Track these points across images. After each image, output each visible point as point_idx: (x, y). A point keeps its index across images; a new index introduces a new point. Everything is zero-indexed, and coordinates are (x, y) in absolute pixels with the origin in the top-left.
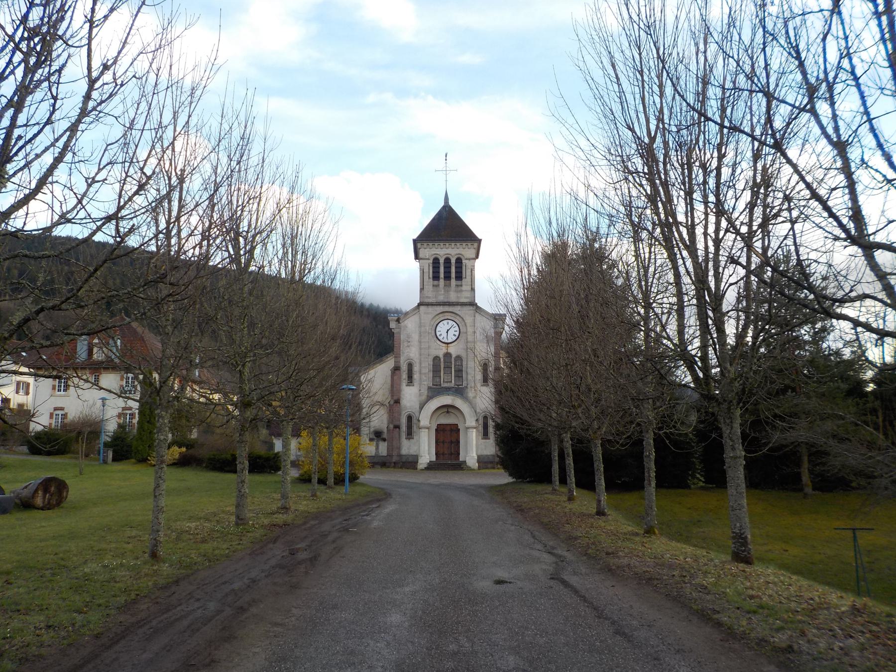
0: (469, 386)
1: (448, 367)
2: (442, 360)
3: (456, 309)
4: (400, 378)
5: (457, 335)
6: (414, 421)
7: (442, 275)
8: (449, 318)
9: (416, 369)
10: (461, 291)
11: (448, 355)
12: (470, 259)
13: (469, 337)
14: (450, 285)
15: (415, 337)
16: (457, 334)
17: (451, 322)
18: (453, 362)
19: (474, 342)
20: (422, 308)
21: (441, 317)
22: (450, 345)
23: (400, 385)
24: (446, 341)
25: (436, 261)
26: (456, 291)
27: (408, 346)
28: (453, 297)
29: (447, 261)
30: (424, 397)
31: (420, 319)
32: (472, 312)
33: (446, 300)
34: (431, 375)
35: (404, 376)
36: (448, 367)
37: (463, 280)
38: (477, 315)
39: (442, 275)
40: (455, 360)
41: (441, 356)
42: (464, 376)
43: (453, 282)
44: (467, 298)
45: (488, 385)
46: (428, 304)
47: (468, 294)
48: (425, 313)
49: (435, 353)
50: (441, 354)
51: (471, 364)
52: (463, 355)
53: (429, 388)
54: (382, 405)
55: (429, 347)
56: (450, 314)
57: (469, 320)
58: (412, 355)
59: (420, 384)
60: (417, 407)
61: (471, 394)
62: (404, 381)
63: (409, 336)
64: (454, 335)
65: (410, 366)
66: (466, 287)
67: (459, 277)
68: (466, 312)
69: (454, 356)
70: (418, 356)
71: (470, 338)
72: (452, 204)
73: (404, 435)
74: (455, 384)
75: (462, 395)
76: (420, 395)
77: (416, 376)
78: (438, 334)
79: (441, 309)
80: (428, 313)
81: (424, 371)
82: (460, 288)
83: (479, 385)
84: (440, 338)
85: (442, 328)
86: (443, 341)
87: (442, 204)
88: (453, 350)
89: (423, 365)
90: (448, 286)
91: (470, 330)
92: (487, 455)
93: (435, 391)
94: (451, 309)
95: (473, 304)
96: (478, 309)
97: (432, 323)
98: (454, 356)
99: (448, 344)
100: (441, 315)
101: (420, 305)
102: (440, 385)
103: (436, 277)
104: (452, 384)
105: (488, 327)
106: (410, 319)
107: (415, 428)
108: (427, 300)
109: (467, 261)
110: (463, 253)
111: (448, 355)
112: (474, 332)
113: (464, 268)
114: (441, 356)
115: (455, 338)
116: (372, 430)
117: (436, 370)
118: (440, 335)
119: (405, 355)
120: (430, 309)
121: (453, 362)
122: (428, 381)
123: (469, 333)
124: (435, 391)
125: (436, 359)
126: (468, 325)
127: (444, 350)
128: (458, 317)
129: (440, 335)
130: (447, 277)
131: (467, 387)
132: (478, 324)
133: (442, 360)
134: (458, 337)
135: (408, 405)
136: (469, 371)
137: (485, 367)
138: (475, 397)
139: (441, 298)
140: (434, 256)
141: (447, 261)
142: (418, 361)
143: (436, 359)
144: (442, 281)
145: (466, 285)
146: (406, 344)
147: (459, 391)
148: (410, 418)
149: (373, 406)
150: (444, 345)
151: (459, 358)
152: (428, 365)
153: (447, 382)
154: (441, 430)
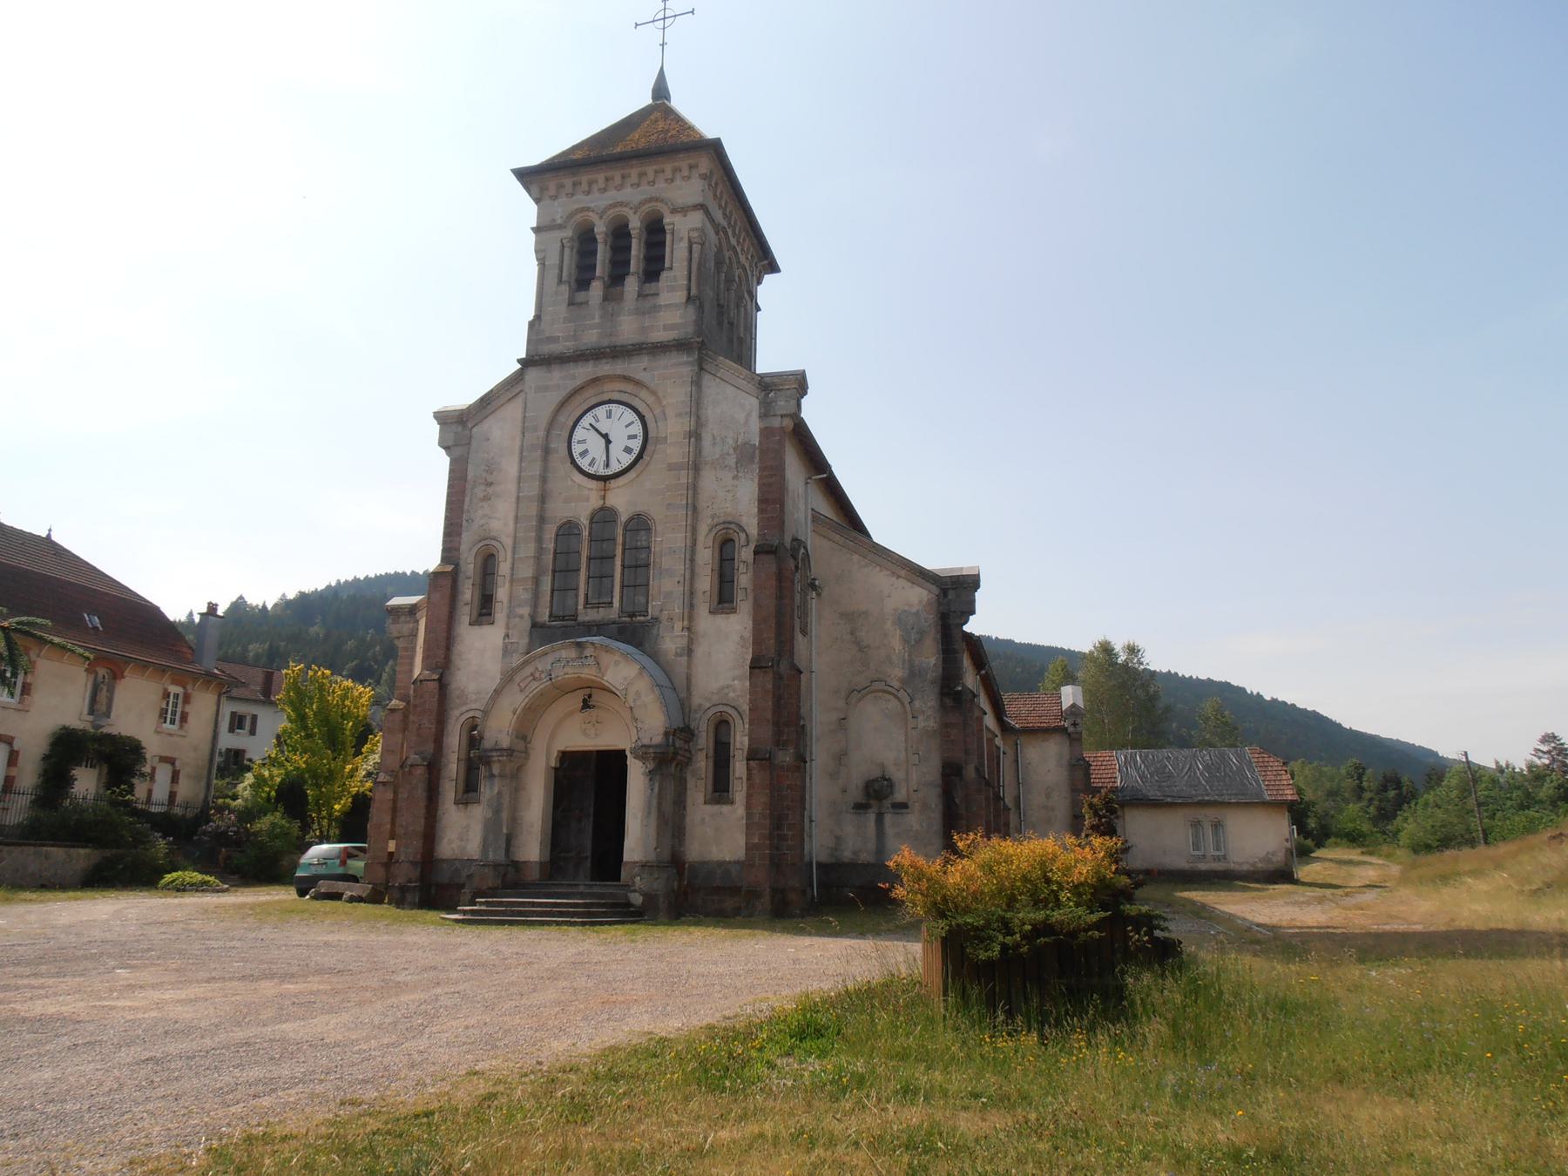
1: (602, 559)
3: (637, 367)
5: (636, 450)
8: (616, 396)
9: (504, 568)
10: (656, 309)
11: (604, 516)
12: (683, 210)
14: (620, 298)
16: (636, 445)
18: (620, 540)
20: (533, 374)
21: (590, 397)
22: (613, 483)
24: (602, 471)
26: (640, 312)
27: (486, 498)
28: (628, 329)
33: (605, 342)
36: (602, 559)
41: (584, 521)
43: (631, 285)
44: (672, 327)
45: (733, 610)
49: (560, 511)
50: (582, 514)
58: (495, 525)
61: (670, 642)
62: (467, 609)
64: (628, 450)
65: (488, 563)
69: (623, 518)
72: (680, 103)
75: (639, 645)
76: (506, 651)
79: (584, 372)
80: (546, 389)
83: (702, 610)
84: (584, 463)
86: (592, 471)
87: (646, 100)
88: (622, 500)
89: (521, 554)
92: (721, 864)
94: (619, 367)
99: (605, 479)
100: (590, 392)
101: (526, 363)
102: (574, 617)
104: (613, 613)
108: (547, 349)
111: (604, 516)
113: (668, 237)
115: (627, 459)
117: (564, 569)
118: (584, 453)
121: (620, 540)
127: (595, 502)
129: (584, 453)
132: (711, 412)
133: (585, 533)
134: (640, 457)
137: (725, 547)
139: (591, 338)
142: (508, 542)
143: (568, 530)
144: (596, 289)
145: (672, 289)
146: (480, 491)
150: (593, 484)
151: (640, 524)
153: (598, 606)
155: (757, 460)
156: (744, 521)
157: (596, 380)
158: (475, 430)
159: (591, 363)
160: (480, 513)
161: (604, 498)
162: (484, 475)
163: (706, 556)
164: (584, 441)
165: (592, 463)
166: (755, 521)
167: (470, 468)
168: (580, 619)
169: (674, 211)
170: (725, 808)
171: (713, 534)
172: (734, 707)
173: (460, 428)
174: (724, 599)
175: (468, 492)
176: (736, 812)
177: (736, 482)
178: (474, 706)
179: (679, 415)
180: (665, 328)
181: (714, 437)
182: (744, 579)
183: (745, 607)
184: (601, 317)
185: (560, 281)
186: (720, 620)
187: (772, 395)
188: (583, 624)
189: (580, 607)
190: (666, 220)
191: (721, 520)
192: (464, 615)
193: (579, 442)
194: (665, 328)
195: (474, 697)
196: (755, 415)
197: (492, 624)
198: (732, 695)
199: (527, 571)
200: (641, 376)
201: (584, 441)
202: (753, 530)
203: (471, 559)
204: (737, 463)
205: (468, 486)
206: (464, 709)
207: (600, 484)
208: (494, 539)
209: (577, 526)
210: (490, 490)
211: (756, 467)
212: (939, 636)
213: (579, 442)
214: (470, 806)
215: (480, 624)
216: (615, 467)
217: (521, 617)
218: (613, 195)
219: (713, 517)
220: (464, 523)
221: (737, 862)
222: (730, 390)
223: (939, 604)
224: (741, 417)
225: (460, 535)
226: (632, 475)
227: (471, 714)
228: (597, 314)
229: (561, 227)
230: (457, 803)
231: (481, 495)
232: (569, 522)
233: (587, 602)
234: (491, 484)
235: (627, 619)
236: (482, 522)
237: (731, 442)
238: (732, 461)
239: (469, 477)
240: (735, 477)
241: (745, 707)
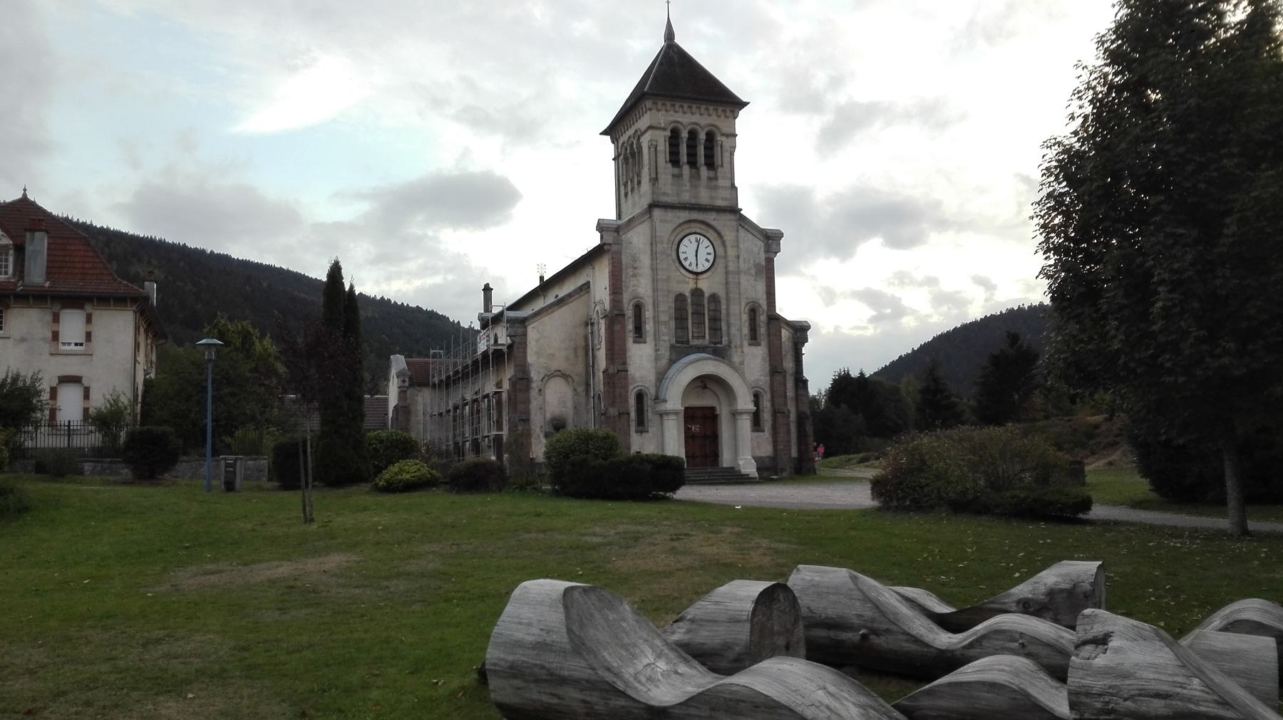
0: (733, 345)
1: (698, 314)
2: (689, 300)
3: (710, 218)
4: (624, 328)
6: (648, 402)
7: (684, 158)
8: (698, 231)
9: (648, 313)
10: (716, 188)
11: (697, 293)
13: (730, 264)
14: (698, 176)
15: (645, 261)
16: (711, 258)
17: (693, 237)
18: (706, 305)
19: (738, 273)
20: (657, 213)
22: (701, 277)
23: (624, 341)
24: (695, 270)
25: (674, 136)
26: (709, 188)
27: (634, 276)
28: (704, 197)
29: (693, 135)
30: (664, 362)
31: (653, 229)
32: (734, 223)
33: (693, 201)
34: (673, 324)
35: (630, 326)
36: (698, 314)
37: (720, 170)
38: (741, 230)
39: (684, 158)
40: (709, 302)
41: (688, 294)
42: (724, 328)
45: (759, 344)
46: (666, 206)
47: (726, 194)
48: (661, 221)
50: (687, 289)
51: (734, 309)
52: (722, 294)
53: (672, 347)
54: (565, 376)
55: (668, 279)
56: (698, 225)
57: (729, 236)
59: (656, 338)
60: (652, 377)
62: (631, 334)
63: (635, 259)
64: (707, 260)
65: (638, 308)
66: (722, 182)
67: (711, 164)
68: (723, 223)
69: (707, 295)
70: (650, 292)
71: (732, 267)
73: (633, 428)
74: (711, 342)
77: (649, 327)
78: (682, 257)
79: (685, 215)
81: (664, 318)
82: (714, 183)
83: (746, 343)
84: (686, 264)
85: (688, 248)
88: (705, 285)
89: (661, 309)
90: (696, 176)
91: (731, 252)
93: (681, 349)
95: (734, 210)
96: (743, 221)
97: (672, 239)
98: (707, 295)
99: (697, 274)
100: (685, 226)
101: (653, 206)
102: (688, 342)
103: (675, 161)
105: (756, 250)
106: (636, 229)
107: (649, 415)
108: (664, 199)
109: (724, 139)
110: (716, 123)
112: (738, 257)
114: (688, 294)
115: (707, 265)
116: (548, 416)
117: (680, 319)
118: (686, 259)
119: (630, 290)
120: (670, 215)
121: (706, 305)
122: (668, 336)
123: (730, 259)
124: (681, 349)
125: (680, 298)
126: (728, 244)
127: (692, 285)
128: (711, 231)
130: (693, 163)
131: (729, 346)
133: (689, 300)
135: (637, 375)
136: (732, 320)
138: (742, 363)
139: (686, 197)
140: (672, 125)
141: (693, 135)
143: (680, 298)
144: (686, 170)
145: (724, 178)
146: (630, 271)
147: (719, 352)
148: (640, 397)
149: (549, 376)
150: (691, 276)
151: (714, 298)
152: (667, 307)
153: (698, 338)
154: (691, 415)
155: (764, 272)
156: (761, 302)
157: (689, 221)
158: (624, 236)
159: (687, 211)
160: (632, 283)
161: (696, 283)
162: (631, 262)
163: (745, 317)
164: (685, 253)
165: (690, 265)
166: (765, 303)
167: (623, 257)
168: (691, 343)
169: (723, 135)
170: (761, 434)
171: (747, 307)
172: (762, 389)
173: (616, 234)
174: (754, 338)
175: (624, 272)
176: (766, 435)
177: (756, 283)
178: (640, 384)
179: (732, 247)
180: (723, 199)
181: (744, 259)
182: (762, 330)
183: (764, 343)
184: (691, 186)
185: (666, 161)
186: (753, 348)
187: (770, 241)
188: (691, 347)
189: (690, 338)
190: (719, 138)
191: (751, 301)
192: (630, 340)
193: (683, 253)
194: (723, 199)
195: (639, 379)
196: (762, 250)
197: (645, 343)
198: (760, 383)
199: (664, 318)
200: (712, 223)
201: (685, 253)
202: (765, 307)
203: (631, 307)
204: (756, 273)
205: (624, 267)
206: (636, 385)
207: (695, 277)
208: (641, 298)
209: (684, 296)
210: (636, 271)
211: (764, 276)
212: (793, 353)
213: (683, 253)
214: (643, 434)
215: (639, 343)
216: (700, 269)
217: (665, 341)
218: (696, 118)
219: (747, 298)
220: (624, 288)
221: (768, 457)
222: (750, 235)
223: (794, 338)
224: (756, 250)
225: (621, 294)
226: (709, 274)
227: (639, 388)
228: (688, 184)
229: (664, 129)
230: (637, 432)
231: (631, 273)
232: (681, 294)
233: (693, 336)
234: (636, 268)
235: (712, 345)
236: (634, 288)
237: (752, 262)
238: (753, 272)
239: (623, 263)
240: (755, 280)
241: (768, 389)
